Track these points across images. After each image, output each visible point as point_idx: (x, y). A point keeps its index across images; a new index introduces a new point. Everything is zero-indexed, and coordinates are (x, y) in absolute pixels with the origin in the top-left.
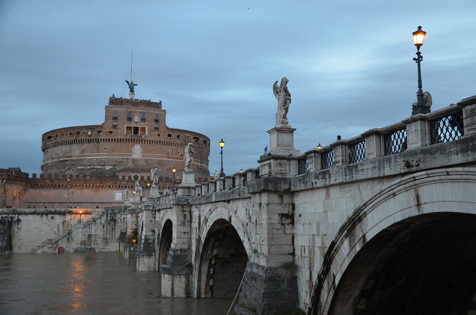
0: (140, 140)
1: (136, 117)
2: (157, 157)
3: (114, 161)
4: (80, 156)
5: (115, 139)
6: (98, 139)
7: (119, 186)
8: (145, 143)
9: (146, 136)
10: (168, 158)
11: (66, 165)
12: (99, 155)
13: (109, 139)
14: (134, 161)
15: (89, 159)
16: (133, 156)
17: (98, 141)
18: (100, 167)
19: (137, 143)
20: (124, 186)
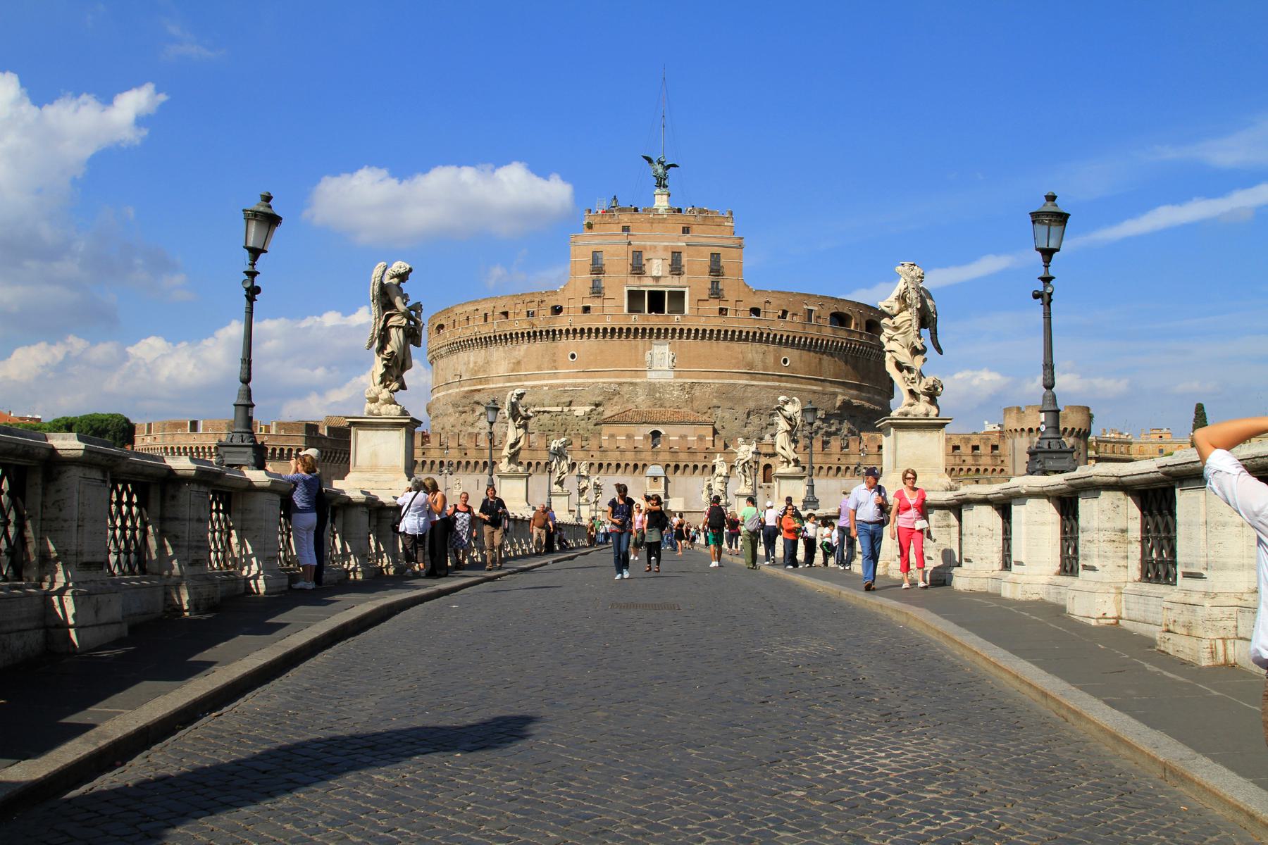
0: (666, 330)
1: (655, 261)
3: (597, 392)
4: (508, 379)
5: (597, 330)
6: (554, 331)
7: (601, 465)
10: (753, 376)
11: (478, 403)
12: (555, 376)
13: (582, 330)
14: (652, 389)
15: (532, 387)
16: (649, 374)
19: (658, 337)
20: (614, 464)
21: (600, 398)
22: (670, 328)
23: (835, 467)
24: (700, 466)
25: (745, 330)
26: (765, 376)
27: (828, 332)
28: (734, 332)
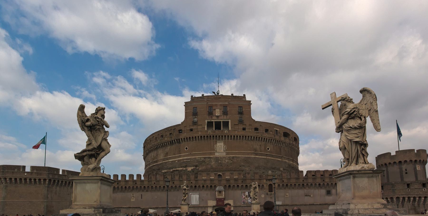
0: (222, 136)
2: (244, 154)
5: (196, 137)
6: (179, 139)
7: (195, 186)
8: (228, 139)
9: (229, 131)
10: (256, 154)
12: (180, 156)
13: (190, 138)
14: (217, 159)
16: (216, 154)
17: (178, 141)
18: (182, 169)
19: (219, 139)
20: (201, 186)
21: (197, 164)
22: (224, 135)
23: (301, 184)
24: (240, 185)
25: (253, 136)
26: (262, 155)
27: (283, 138)
28: (249, 137)
